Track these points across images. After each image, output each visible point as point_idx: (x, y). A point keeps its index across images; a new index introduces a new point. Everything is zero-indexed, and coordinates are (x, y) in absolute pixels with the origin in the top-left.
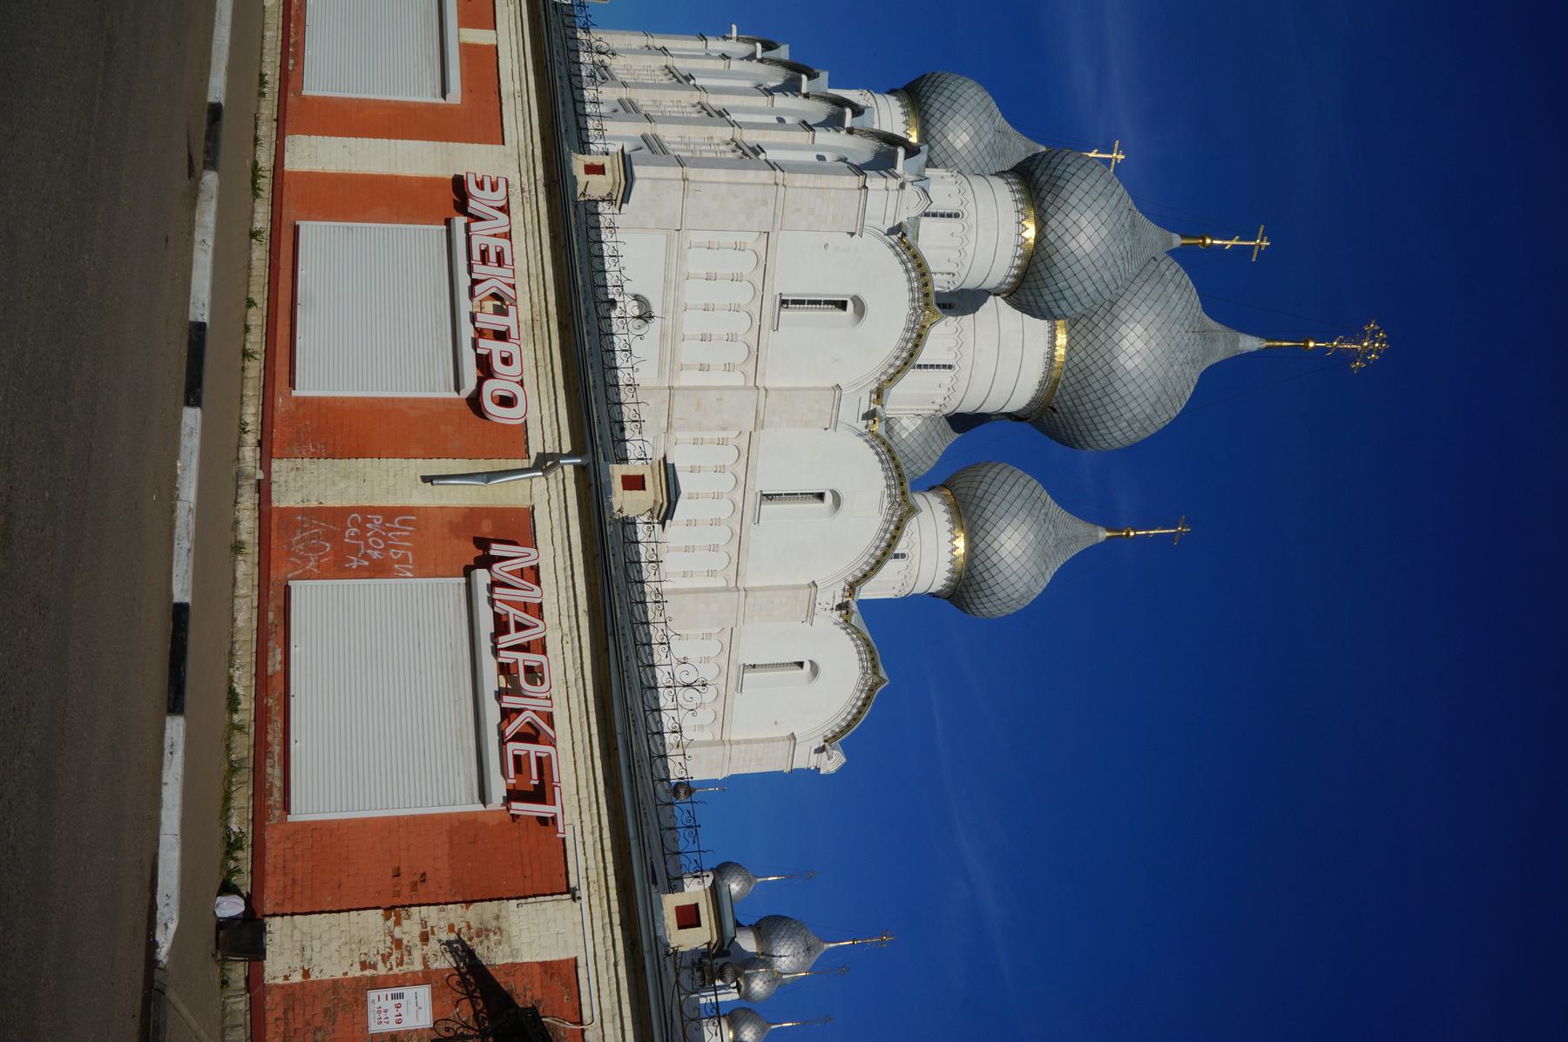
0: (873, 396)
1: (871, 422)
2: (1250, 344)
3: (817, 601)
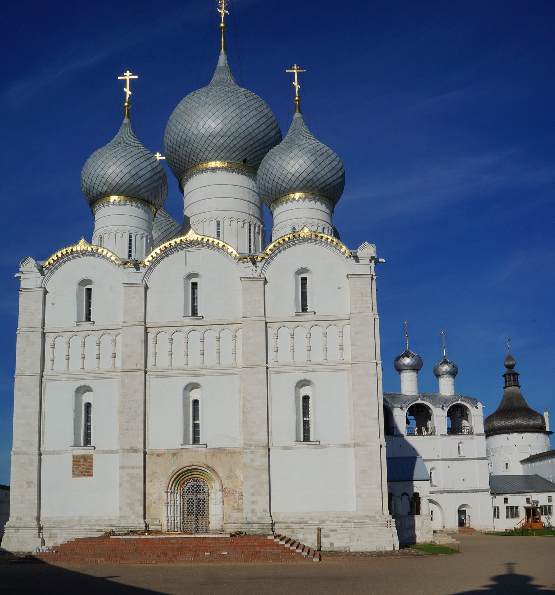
0: (126, 267)
1: (141, 265)
2: (222, 60)
3: (251, 276)
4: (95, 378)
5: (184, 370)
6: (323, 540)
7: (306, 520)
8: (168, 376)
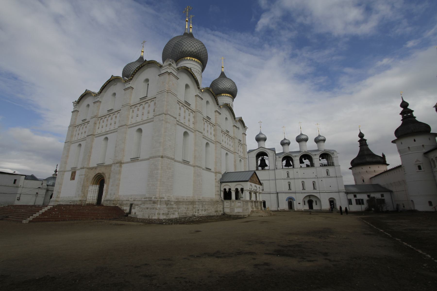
4: (82, 141)
5: (104, 132)
6: (133, 211)
7: (129, 199)
8: (100, 136)
